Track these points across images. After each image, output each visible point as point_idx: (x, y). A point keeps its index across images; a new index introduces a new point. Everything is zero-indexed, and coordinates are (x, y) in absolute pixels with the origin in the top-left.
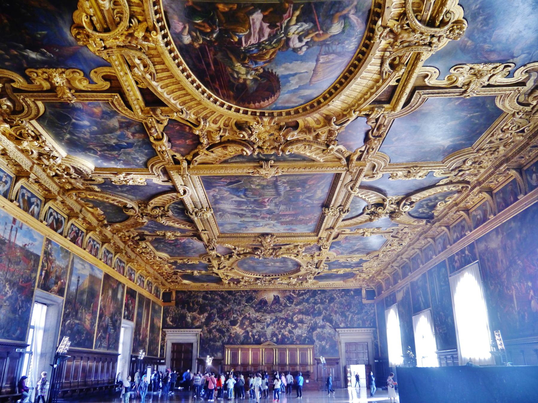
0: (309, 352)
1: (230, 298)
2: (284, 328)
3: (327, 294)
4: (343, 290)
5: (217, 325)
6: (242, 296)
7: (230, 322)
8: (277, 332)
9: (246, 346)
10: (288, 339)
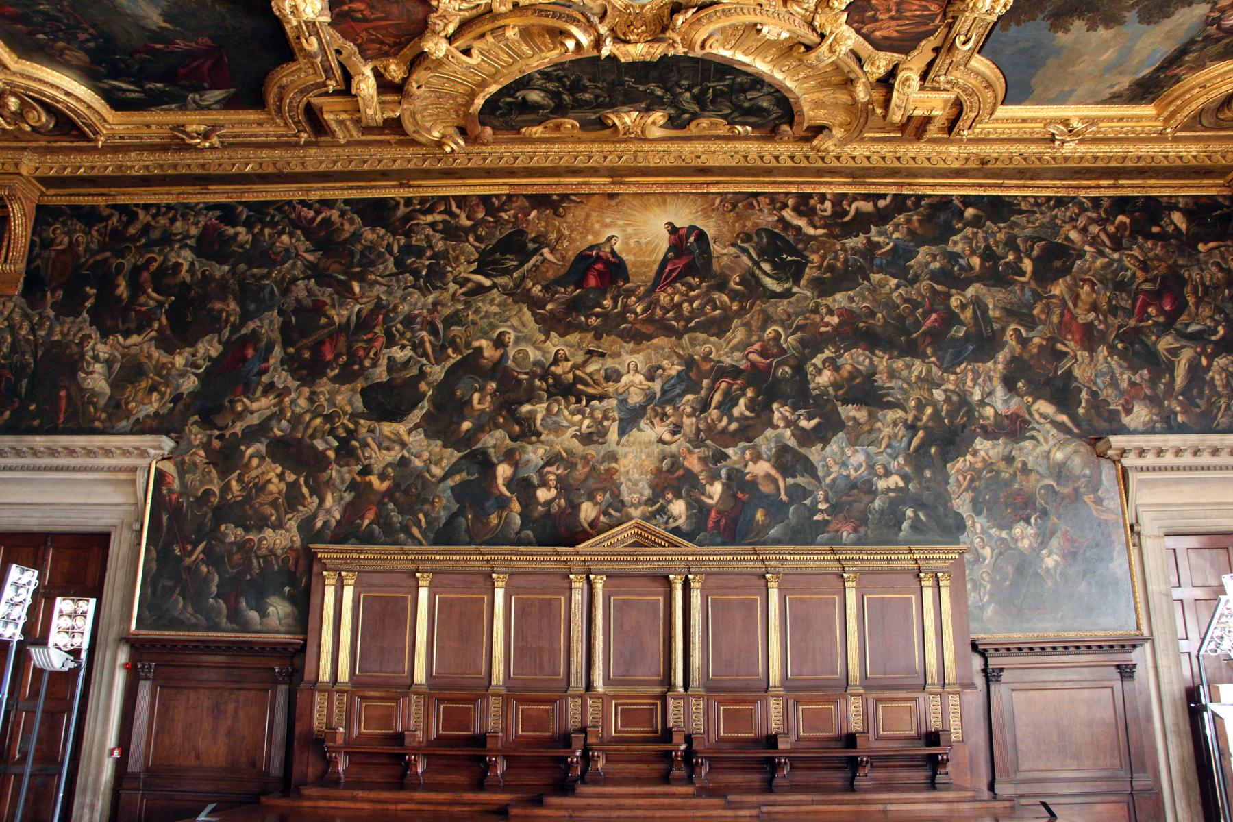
0: (928, 594)
1: (371, 248)
2: (747, 432)
3: (1026, 227)
4: (1121, 204)
5: (279, 415)
6: (452, 232)
7: (364, 392)
8: (693, 464)
9: (468, 557)
10: (776, 509)
